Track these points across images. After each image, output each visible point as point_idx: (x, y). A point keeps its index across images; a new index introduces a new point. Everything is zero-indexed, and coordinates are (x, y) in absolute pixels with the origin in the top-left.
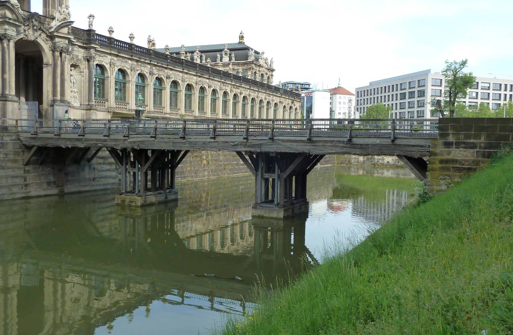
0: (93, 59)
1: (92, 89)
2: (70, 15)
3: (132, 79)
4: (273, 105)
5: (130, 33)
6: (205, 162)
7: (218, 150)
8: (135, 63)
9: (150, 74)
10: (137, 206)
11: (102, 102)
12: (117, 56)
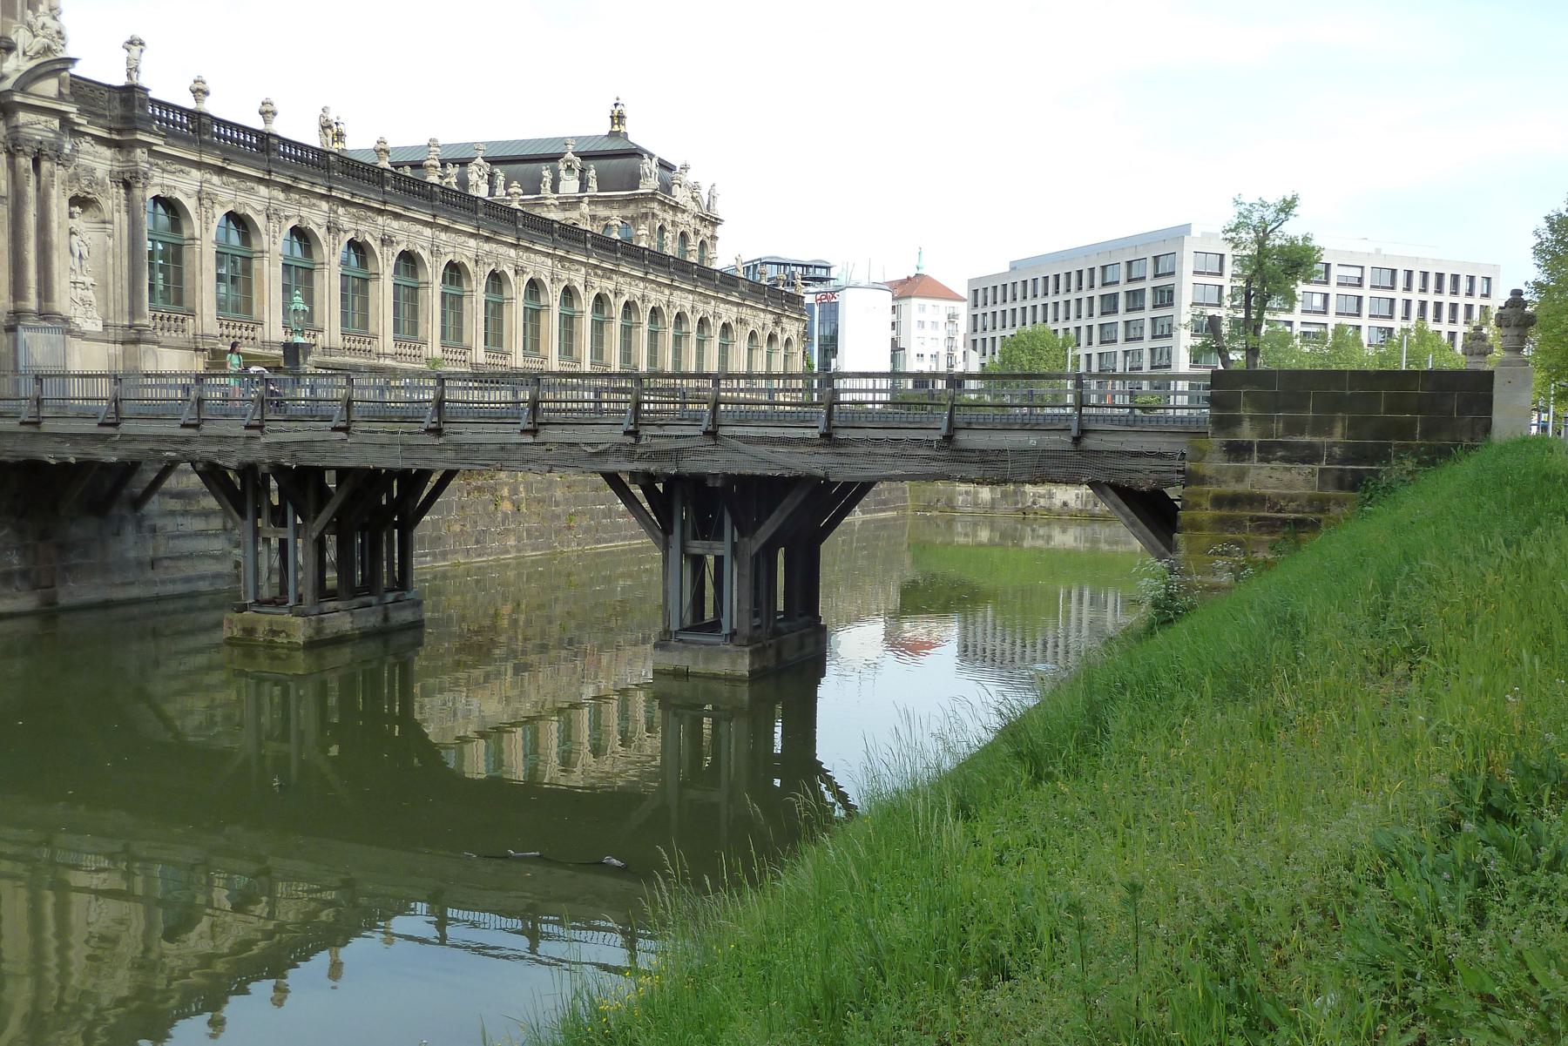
0: (143, 180)
1: (141, 278)
2: (63, 39)
3: (272, 245)
4: (719, 330)
5: (264, 100)
6: (507, 506)
7: (547, 468)
8: (282, 196)
9: (328, 228)
10: (292, 647)
11: (176, 319)
12: (221, 171)
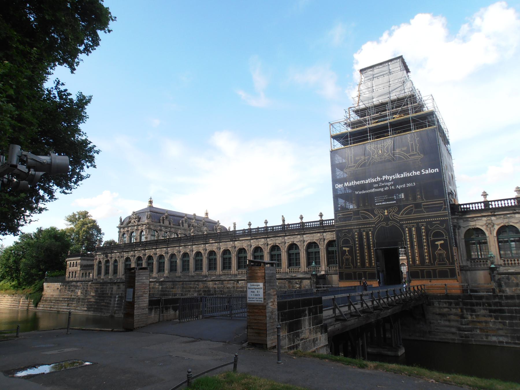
12: (495, 215)
